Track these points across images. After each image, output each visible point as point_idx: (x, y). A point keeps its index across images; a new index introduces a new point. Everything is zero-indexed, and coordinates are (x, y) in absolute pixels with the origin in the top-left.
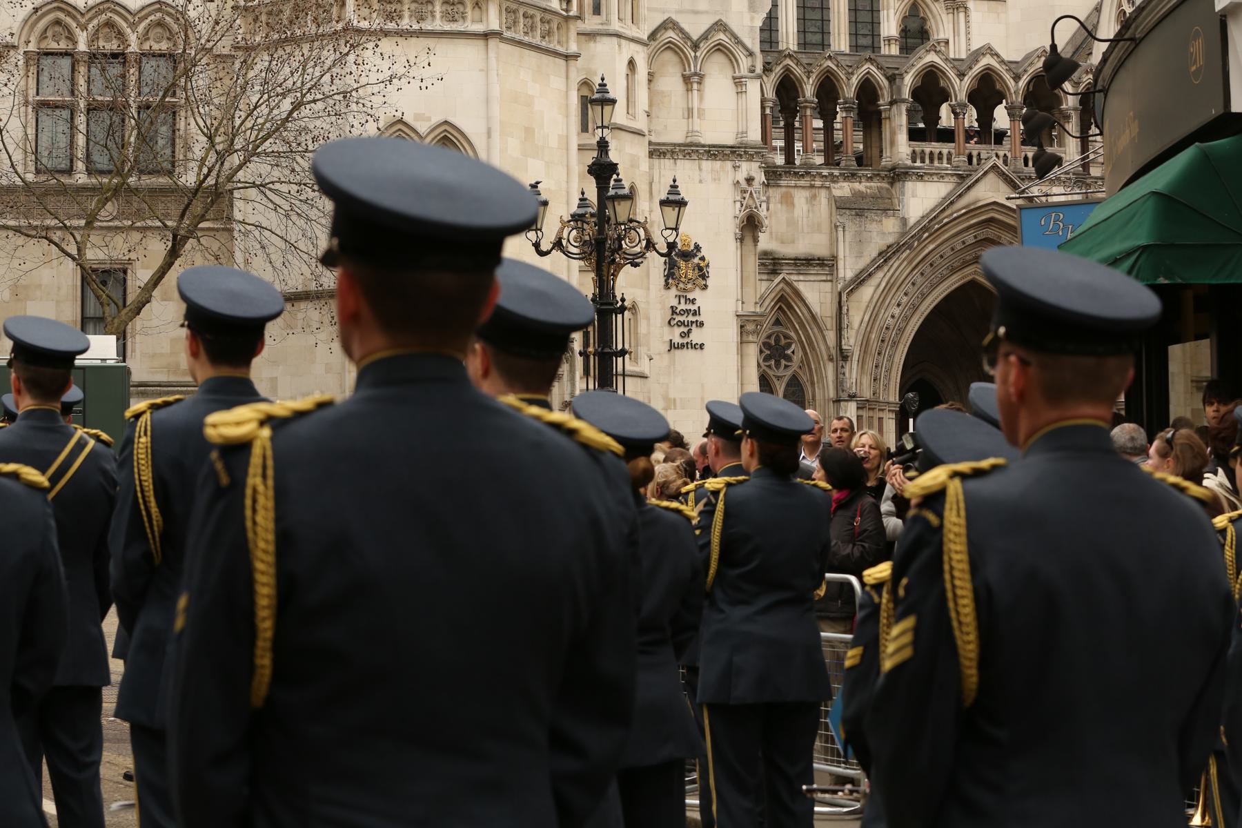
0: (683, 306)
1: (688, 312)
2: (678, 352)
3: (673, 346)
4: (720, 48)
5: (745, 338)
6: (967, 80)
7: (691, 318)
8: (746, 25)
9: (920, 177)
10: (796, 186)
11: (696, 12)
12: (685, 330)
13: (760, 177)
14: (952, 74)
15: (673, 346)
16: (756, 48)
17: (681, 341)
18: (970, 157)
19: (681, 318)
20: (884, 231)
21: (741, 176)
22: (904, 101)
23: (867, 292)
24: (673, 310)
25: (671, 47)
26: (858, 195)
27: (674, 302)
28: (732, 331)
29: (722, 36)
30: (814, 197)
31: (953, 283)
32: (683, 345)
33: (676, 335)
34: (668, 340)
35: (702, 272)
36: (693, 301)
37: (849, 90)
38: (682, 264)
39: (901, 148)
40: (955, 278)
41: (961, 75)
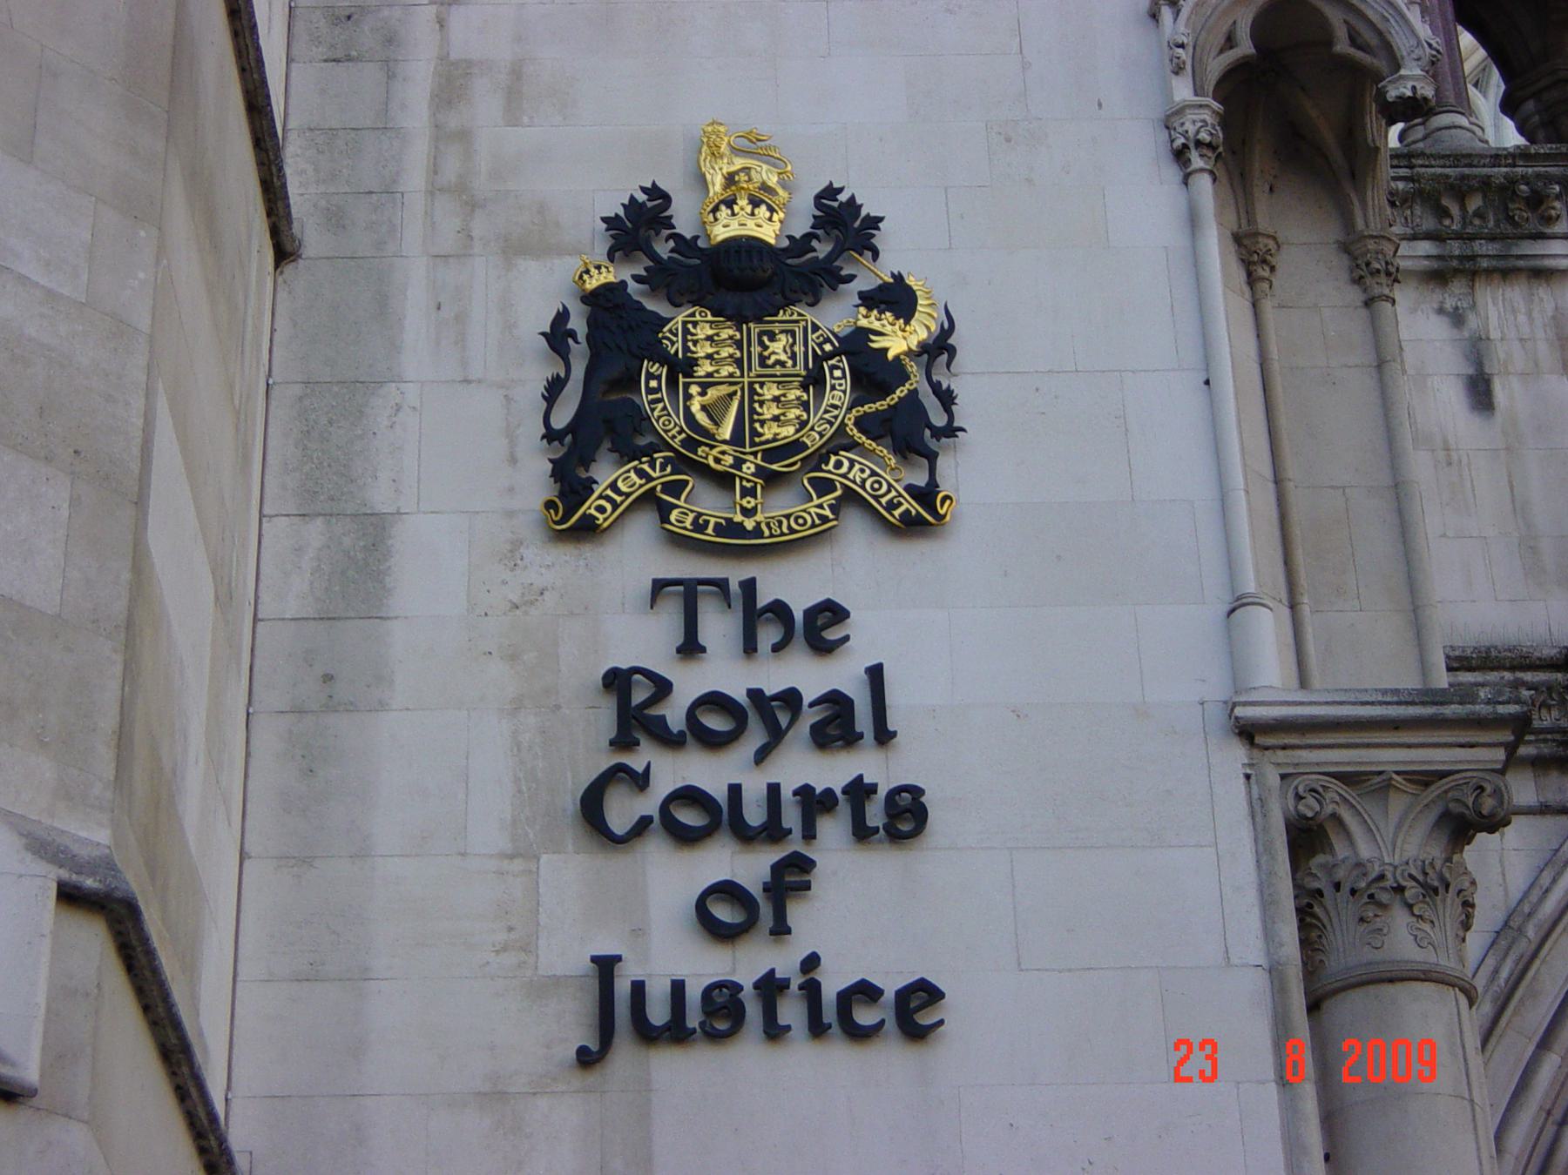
0: (725, 671)
2: (679, 1073)
3: (622, 1019)
5: (1347, 948)
7: (803, 767)
12: (750, 868)
15: (622, 1019)
17: (705, 965)
19: (710, 773)
24: (633, 704)
27: (646, 641)
28: (1205, 883)
32: (723, 1013)
33: (653, 908)
34: (568, 955)
35: (905, 415)
38: (702, 334)
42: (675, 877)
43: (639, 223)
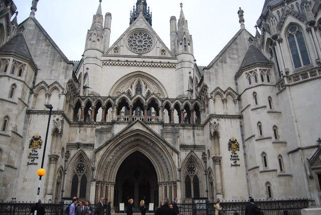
0: (33, 153)
1: (35, 154)
3: (28, 164)
4: (56, 88)
6: (133, 101)
8: (63, 81)
9: (118, 123)
10: (87, 127)
11: (50, 79)
12: (33, 159)
13: (61, 119)
14: (129, 99)
15: (28, 164)
16: (65, 88)
18: (133, 119)
20: (107, 137)
21: (55, 119)
22: (116, 105)
23: (101, 152)
25: (43, 88)
26: (102, 128)
27: (31, 152)
29: (56, 85)
30: (92, 130)
31: (131, 151)
32: (31, 164)
36: (37, 151)
37: (104, 104)
40: (132, 150)
41: (131, 99)
42: (31, 159)
43: (34, 137)
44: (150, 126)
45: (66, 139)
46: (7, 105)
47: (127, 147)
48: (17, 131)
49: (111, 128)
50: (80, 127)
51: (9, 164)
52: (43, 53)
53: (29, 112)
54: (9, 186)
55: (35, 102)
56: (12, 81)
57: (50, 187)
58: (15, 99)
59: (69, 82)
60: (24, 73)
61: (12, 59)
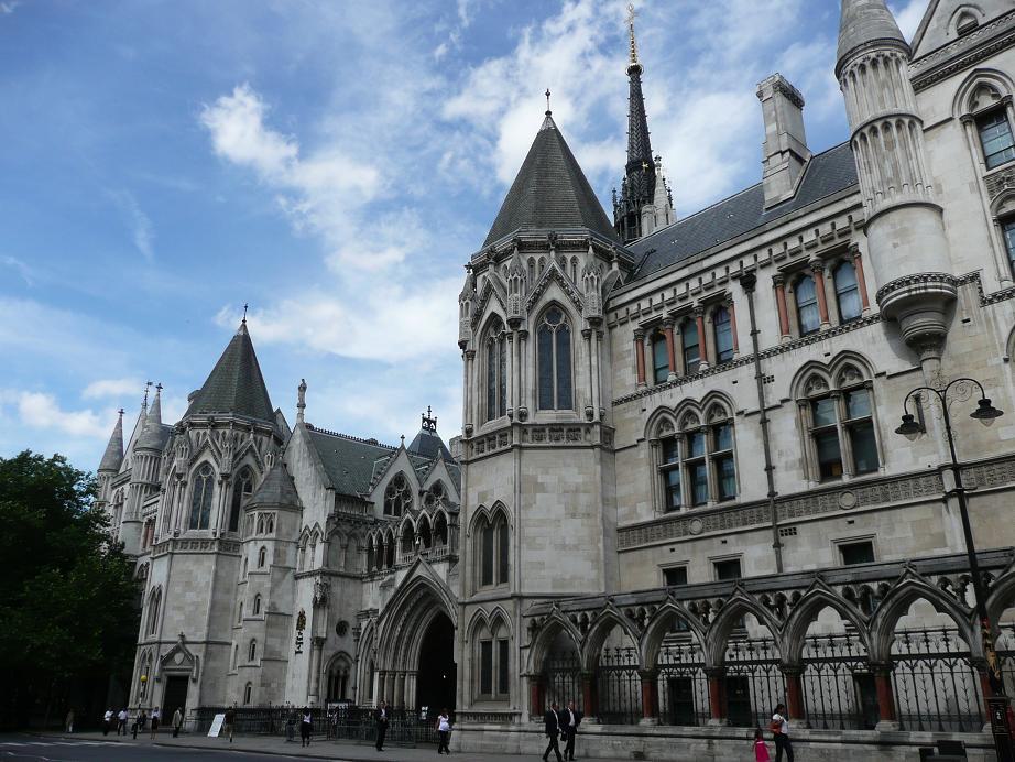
3: (296, 653)
8: (323, 522)
39: (399, 557)
44: (435, 567)
45: (349, 605)
46: (257, 579)
47: (420, 609)
48: (276, 608)
49: (393, 580)
50: (372, 581)
51: (267, 657)
52: (307, 479)
53: (297, 578)
54: (274, 685)
55: (303, 561)
56: (260, 544)
57: (313, 685)
58: (267, 568)
59: (330, 518)
60: (275, 527)
61: (256, 512)
